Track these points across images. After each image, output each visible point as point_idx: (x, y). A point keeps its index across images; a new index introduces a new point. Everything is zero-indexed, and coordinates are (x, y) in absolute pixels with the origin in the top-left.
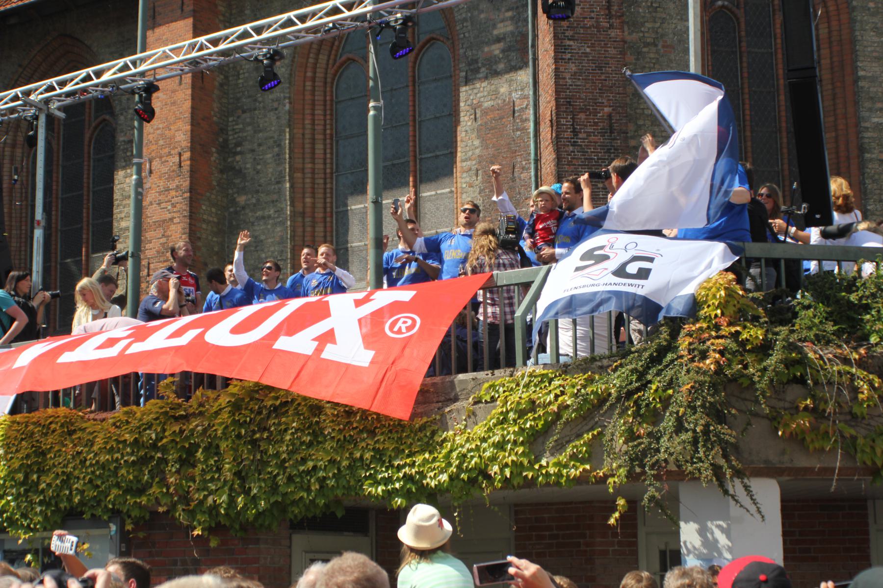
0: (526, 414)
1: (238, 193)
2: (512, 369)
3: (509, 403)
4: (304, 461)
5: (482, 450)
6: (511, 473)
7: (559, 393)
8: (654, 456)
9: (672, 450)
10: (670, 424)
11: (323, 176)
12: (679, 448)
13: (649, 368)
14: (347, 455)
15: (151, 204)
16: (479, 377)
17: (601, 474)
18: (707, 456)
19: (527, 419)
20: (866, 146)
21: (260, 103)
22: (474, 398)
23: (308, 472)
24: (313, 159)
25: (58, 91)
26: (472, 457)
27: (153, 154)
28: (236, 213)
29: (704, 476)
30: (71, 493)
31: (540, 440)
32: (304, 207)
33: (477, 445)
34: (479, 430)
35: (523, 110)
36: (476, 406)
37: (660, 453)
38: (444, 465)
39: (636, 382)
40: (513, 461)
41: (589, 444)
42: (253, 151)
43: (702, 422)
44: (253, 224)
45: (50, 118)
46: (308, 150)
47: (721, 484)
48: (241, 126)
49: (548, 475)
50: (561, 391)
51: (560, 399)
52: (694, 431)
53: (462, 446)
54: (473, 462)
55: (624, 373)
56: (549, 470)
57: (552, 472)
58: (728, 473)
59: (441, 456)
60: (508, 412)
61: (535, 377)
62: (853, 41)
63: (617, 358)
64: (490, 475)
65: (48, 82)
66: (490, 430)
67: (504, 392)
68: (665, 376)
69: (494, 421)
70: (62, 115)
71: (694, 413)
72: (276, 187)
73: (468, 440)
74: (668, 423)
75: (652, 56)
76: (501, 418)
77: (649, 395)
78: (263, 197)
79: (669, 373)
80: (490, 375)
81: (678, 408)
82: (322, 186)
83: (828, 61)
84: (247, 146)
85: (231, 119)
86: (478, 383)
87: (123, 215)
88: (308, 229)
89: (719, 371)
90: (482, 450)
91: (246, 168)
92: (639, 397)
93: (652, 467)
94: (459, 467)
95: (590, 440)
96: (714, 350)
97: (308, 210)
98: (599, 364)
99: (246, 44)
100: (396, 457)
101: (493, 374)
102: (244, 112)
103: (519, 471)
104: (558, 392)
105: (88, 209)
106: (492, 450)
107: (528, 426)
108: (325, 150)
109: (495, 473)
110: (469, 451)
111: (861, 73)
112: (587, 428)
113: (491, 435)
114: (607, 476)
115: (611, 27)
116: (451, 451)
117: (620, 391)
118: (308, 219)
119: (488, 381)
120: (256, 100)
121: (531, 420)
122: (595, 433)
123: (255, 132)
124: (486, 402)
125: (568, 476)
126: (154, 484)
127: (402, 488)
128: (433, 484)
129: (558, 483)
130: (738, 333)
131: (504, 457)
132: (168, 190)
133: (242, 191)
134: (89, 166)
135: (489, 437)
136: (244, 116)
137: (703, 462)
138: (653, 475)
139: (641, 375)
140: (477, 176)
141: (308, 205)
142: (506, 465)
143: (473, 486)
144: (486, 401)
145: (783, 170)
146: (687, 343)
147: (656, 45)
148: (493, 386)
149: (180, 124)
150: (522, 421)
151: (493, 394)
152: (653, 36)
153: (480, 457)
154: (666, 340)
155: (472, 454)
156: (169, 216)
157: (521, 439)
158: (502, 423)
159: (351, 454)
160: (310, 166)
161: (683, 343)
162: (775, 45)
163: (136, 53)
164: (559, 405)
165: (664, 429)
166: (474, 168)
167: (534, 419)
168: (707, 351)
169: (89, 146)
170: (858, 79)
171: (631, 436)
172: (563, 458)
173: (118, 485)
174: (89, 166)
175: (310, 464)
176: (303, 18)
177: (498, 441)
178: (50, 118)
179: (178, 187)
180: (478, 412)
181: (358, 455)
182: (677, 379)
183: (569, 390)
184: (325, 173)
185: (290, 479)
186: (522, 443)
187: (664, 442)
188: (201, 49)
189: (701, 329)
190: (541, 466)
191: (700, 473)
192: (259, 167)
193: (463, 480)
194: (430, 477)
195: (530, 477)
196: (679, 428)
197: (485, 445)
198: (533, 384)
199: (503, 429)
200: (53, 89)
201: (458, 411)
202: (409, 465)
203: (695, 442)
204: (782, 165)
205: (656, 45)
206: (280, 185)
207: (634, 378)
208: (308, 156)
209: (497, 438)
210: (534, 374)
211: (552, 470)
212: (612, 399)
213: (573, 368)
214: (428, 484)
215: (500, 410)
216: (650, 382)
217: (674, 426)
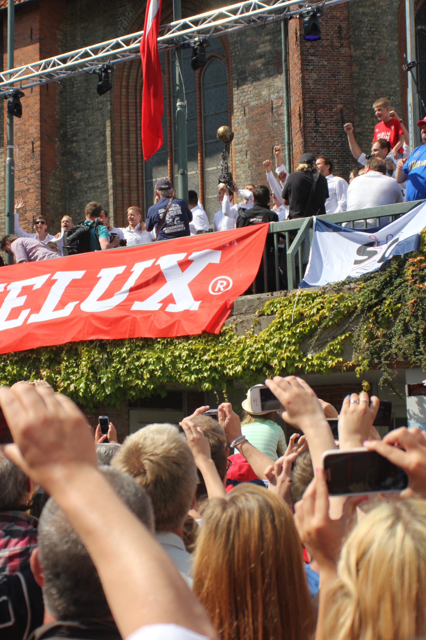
2: (285, 291)
3: (284, 315)
4: (138, 358)
5: (265, 349)
6: (287, 364)
7: (320, 308)
8: (388, 351)
9: (401, 347)
10: (399, 328)
11: (135, 157)
12: (406, 345)
13: (384, 289)
14: (169, 354)
16: (262, 297)
17: (351, 364)
19: (298, 326)
21: (89, 105)
22: (259, 312)
23: (141, 366)
26: (259, 354)
28: (74, 184)
32: (123, 179)
33: (262, 345)
34: (263, 335)
35: (279, 107)
36: (261, 318)
37: (392, 348)
38: (238, 360)
39: (375, 299)
40: (287, 356)
41: (342, 343)
42: (85, 140)
43: (422, 326)
44: (86, 192)
46: (124, 139)
48: (76, 122)
49: (312, 365)
50: (321, 306)
51: (321, 312)
52: (417, 333)
53: (251, 346)
54: (259, 357)
55: (366, 293)
56: (313, 362)
57: (315, 363)
59: (236, 353)
60: (283, 321)
63: (360, 282)
66: (271, 334)
67: (281, 307)
68: (396, 295)
69: (274, 328)
71: (417, 320)
73: (255, 342)
74: (398, 327)
75: (371, 66)
76: (279, 326)
77: (384, 308)
79: (398, 292)
80: (270, 296)
81: (405, 317)
82: (135, 164)
84: (81, 136)
85: (68, 117)
86: (262, 302)
88: (126, 195)
90: (265, 349)
91: (80, 152)
92: (377, 310)
93: (386, 359)
94: (249, 361)
95: (342, 341)
97: (125, 182)
98: (348, 286)
99: (87, 62)
100: (205, 354)
101: (272, 295)
102: (78, 111)
103: (292, 363)
106: (272, 348)
107: (298, 331)
109: (275, 365)
110: (257, 349)
112: (340, 332)
113: (272, 338)
115: (342, 46)
116: (243, 350)
117: (363, 306)
119: (269, 300)
120: (86, 103)
121: (300, 327)
122: (347, 335)
124: (268, 315)
125: (327, 366)
126: (31, 376)
127: (209, 376)
129: (319, 371)
131: (281, 353)
132: (25, 168)
133: (78, 169)
136: (78, 114)
137: (423, 355)
138: (387, 364)
140: (246, 155)
142: (283, 359)
143: (259, 374)
144: (267, 314)
147: (374, 59)
148: (272, 304)
149: (32, 121)
150: (294, 328)
151: (272, 309)
152: (372, 52)
153: (264, 353)
154: (395, 269)
155: (258, 351)
156: (26, 187)
157: (294, 340)
159: (173, 353)
160: (126, 150)
163: (6, 70)
165: (395, 331)
166: (244, 149)
171: (371, 337)
172: (324, 353)
175: (143, 360)
177: (277, 342)
180: (262, 322)
181: (177, 353)
182: (404, 296)
183: (327, 305)
184: (137, 155)
185: (129, 371)
186: (294, 344)
187: (395, 341)
190: (308, 360)
191: (421, 363)
192: (90, 151)
193: (252, 370)
194: (229, 368)
195: (300, 367)
196: (406, 331)
197: (267, 345)
198: (301, 301)
201: (248, 321)
203: (417, 341)
205: (374, 59)
208: (124, 143)
209: (276, 340)
211: (315, 362)
212: (358, 311)
213: (330, 290)
214: (227, 373)
215: (278, 320)
216: (385, 299)
217: (402, 330)
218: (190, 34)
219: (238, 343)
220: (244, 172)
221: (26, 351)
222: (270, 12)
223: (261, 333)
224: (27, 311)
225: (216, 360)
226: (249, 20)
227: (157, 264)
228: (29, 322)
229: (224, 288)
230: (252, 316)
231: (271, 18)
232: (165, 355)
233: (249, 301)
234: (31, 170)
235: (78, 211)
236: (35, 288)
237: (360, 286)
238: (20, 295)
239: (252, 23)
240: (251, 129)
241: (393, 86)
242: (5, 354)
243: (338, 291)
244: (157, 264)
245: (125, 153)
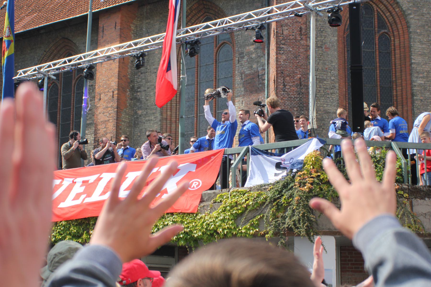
0: (234, 208)
1: (138, 109)
3: (227, 203)
6: (227, 232)
7: (247, 199)
10: (290, 213)
11: (175, 102)
13: (283, 190)
14: (162, 223)
15: (100, 113)
16: (216, 192)
17: (263, 233)
18: (303, 226)
20: (415, 93)
21: (149, 70)
22: (213, 201)
25: (53, 68)
26: (212, 225)
28: (137, 118)
29: (302, 234)
30: (51, 237)
31: (239, 218)
32: (167, 116)
33: (213, 220)
34: (215, 214)
38: (200, 228)
41: (258, 220)
42: (145, 91)
43: (302, 212)
44: (144, 123)
45: (49, 78)
47: (310, 238)
48: (140, 80)
49: (241, 232)
50: (248, 198)
51: (247, 202)
54: (212, 227)
58: (312, 234)
59: (199, 224)
60: (226, 207)
61: (238, 192)
62: (410, 47)
63: (271, 185)
64: (218, 233)
65: (48, 63)
66: (219, 214)
67: (226, 198)
69: (221, 210)
70: (54, 78)
74: (289, 212)
75: (320, 52)
77: (282, 200)
78: (149, 111)
79: (291, 191)
82: (175, 107)
83: (399, 56)
84: (142, 89)
85: (136, 77)
88: (169, 126)
89: (311, 190)
91: (142, 99)
95: (259, 219)
96: (309, 183)
97: (169, 117)
99: (130, 50)
101: (222, 191)
102: (142, 73)
103: (230, 231)
104: (247, 198)
105: (73, 115)
107: (234, 212)
109: (220, 232)
110: (211, 222)
111: (413, 61)
112: (258, 214)
114: (265, 234)
115: (302, 39)
116: (203, 222)
117: (271, 199)
119: (219, 194)
120: (147, 69)
121: (236, 210)
122: (262, 216)
123: (146, 82)
125: (249, 234)
126: (84, 234)
127: (183, 237)
128: (196, 236)
130: (319, 176)
131: (224, 225)
132: (107, 107)
133: (140, 108)
134: (74, 96)
135: (219, 217)
136: (142, 75)
137: (302, 229)
139: (280, 192)
140: (242, 104)
142: (225, 229)
143: (212, 237)
146: (298, 179)
147: (322, 48)
149: (113, 78)
150: (231, 211)
153: (215, 225)
156: (107, 119)
158: (224, 211)
161: (297, 179)
163: (85, 52)
164: (247, 204)
165: (288, 214)
167: (237, 210)
168: (306, 183)
169: (74, 87)
172: (248, 226)
173: (70, 234)
174: (74, 96)
176: (154, 40)
178: (49, 78)
181: (166, 223)
182: (293, 194)
183: (250, 198)
184: (176, 101)
187: (287, 220)
188: (112, 50)
189: (304, 174)
190: (239, 229)
191: (301, 233)
192: (147, 98)
194: (195, 233)
195: (234, 233)
197: (217, 220)
198: (237, 195)
199: (225, 214)
200: (51, 67)
201: (208, 206)
202: (186, 228)
203: (299, 220)
205: (322, 48)
207: (277, 193)
209: (221, 218)
210: (238, 191)
211: (243, 231)
214: (194, 236)
216: (283, 195)
218: (189, 37)
219: (201, 218)
221: (82, 219)
222: (235, 25)
223: (214, 213)
224: (85, 196)
225: (188, 227)
226: (224, 29)
227: (159, 170)
228: (84, 202)
229: (197, 186)
230: (210, 203)
231: (236, 29)
232: (159, 224)
233: (209, 194)
235: (139, 134)
236: (90, 182)
237: (270, 188)
238: (81, 186)
239: (225, 31)
241: (333, 64)
242: (70, 220)
243: (258, 190)
244: (159, 170)
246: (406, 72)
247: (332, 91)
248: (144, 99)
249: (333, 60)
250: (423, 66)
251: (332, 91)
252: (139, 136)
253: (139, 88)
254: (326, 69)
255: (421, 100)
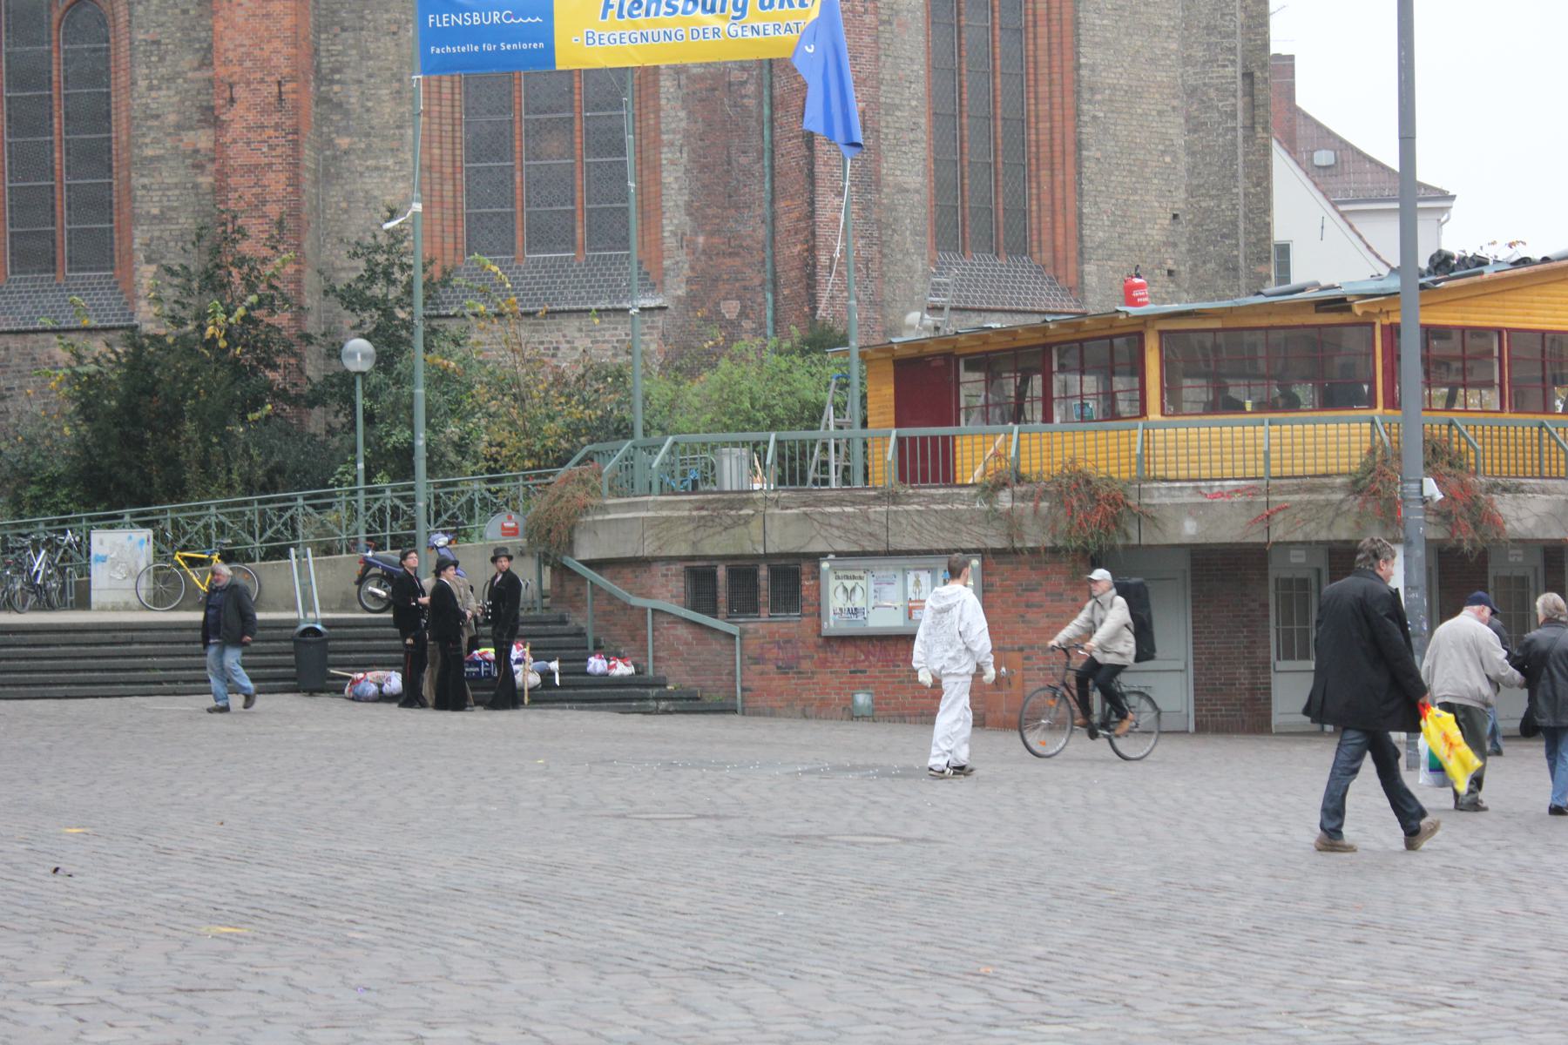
1: (337, 133)
11: (450, 121)
15: (234, 141)
20: (1084, 142)
21: (369, 22)
24: (440, 99)
27: (235, 78)
28: (335, 158)
32: (431, 159)
35: (743, 84)
42: (360, 82)
44: (361, 174)
46: (434, 89)
48: (340, 48)
62: (1077, 24)
72: (397, 132)
75: (887, 35)
78: (376, 142)
82: (450, 134)
83: (1046, 41)
84: (349, 74)
85: (323, 36)
87: (148, 140)
88: (437, 187)
91: (348, 103)
97: (436, 164)
102: (344, 30)
105: (60, 117)
108: (453, 88)
111: (1083, 60)
115: (866, 11)
118: (436, 175)
120: (362, 18)
123: (362, 58)
132: (263, 127)
133: (346, 131)
134: (59, 58)
136: (344, 35)
140: (681, 152)
141: (437, 157)
145: (996, 162)
147: (891, 24)
149: (277, 44)
152: (889, 12)
156: (266, 161)
160: (437, 108)
162: (993, 17)
166: (677, 143)
169: (58, 31)
170: (1078, 67)
174: (59, 58)
179: (277, 127)
184: (453, 119)
192: (370, 104)
204: (995, 156)
205: (891, 24)
206: (402, 131)
208: (435, 96)
220: (677, 179)
234: (276, 130)
235: (344, 205)
240: (690, 113)
241: (915, 67)
245: (435, 114)
246: (1062, 85)
247: (912, 136)
248: (356, 106)
249: (914, 56)
250: (1104, 74)
251: (912, 136)
252: (346, 211)
253: (334, 71)
254: (900, 79)
255: (1098, 159)
